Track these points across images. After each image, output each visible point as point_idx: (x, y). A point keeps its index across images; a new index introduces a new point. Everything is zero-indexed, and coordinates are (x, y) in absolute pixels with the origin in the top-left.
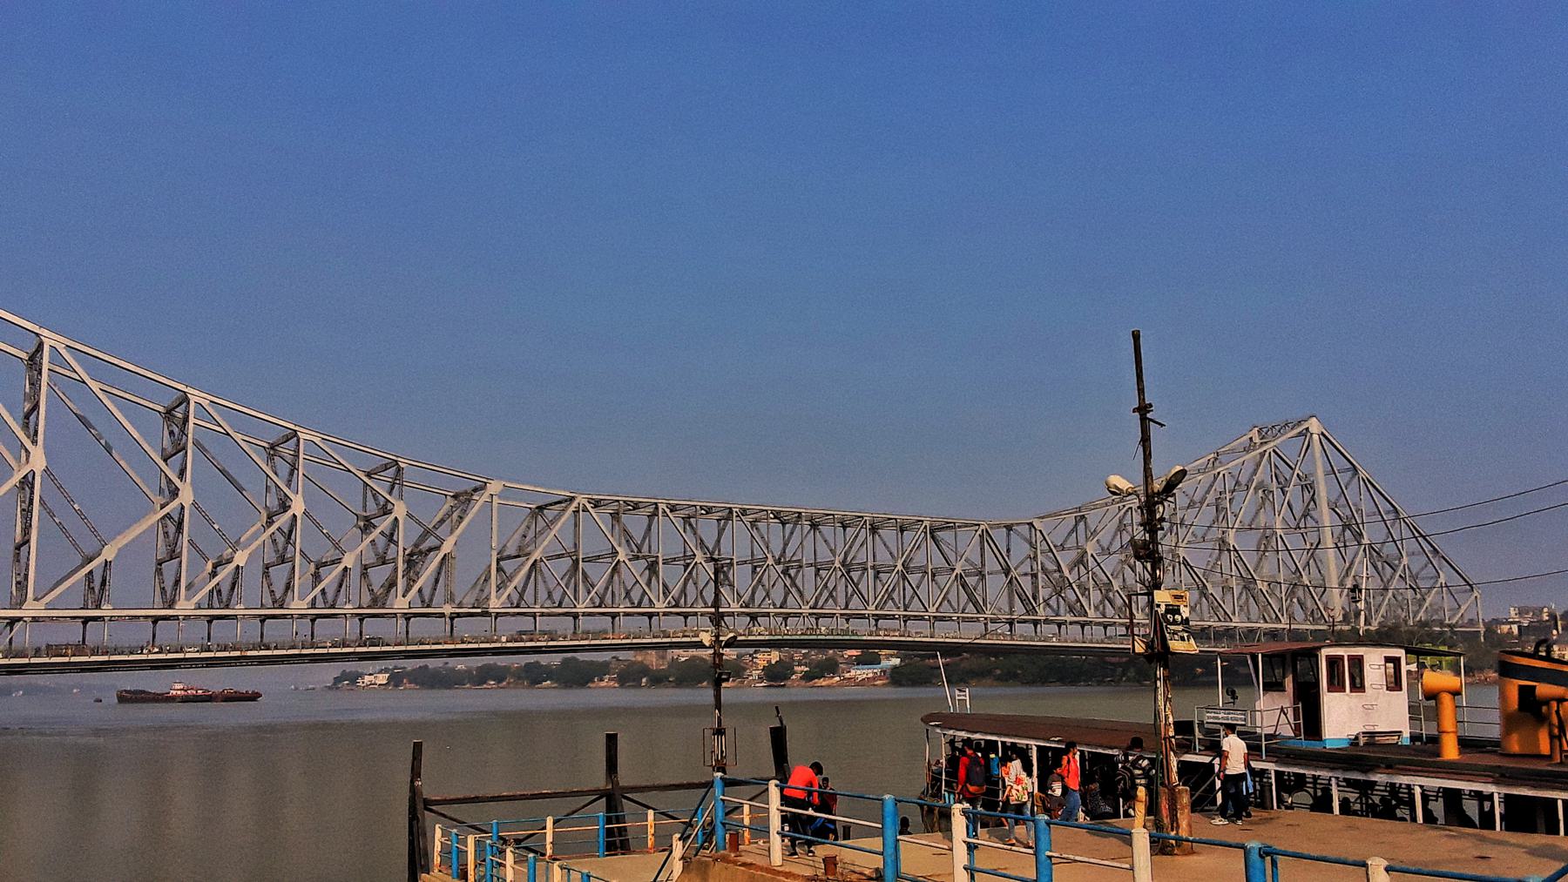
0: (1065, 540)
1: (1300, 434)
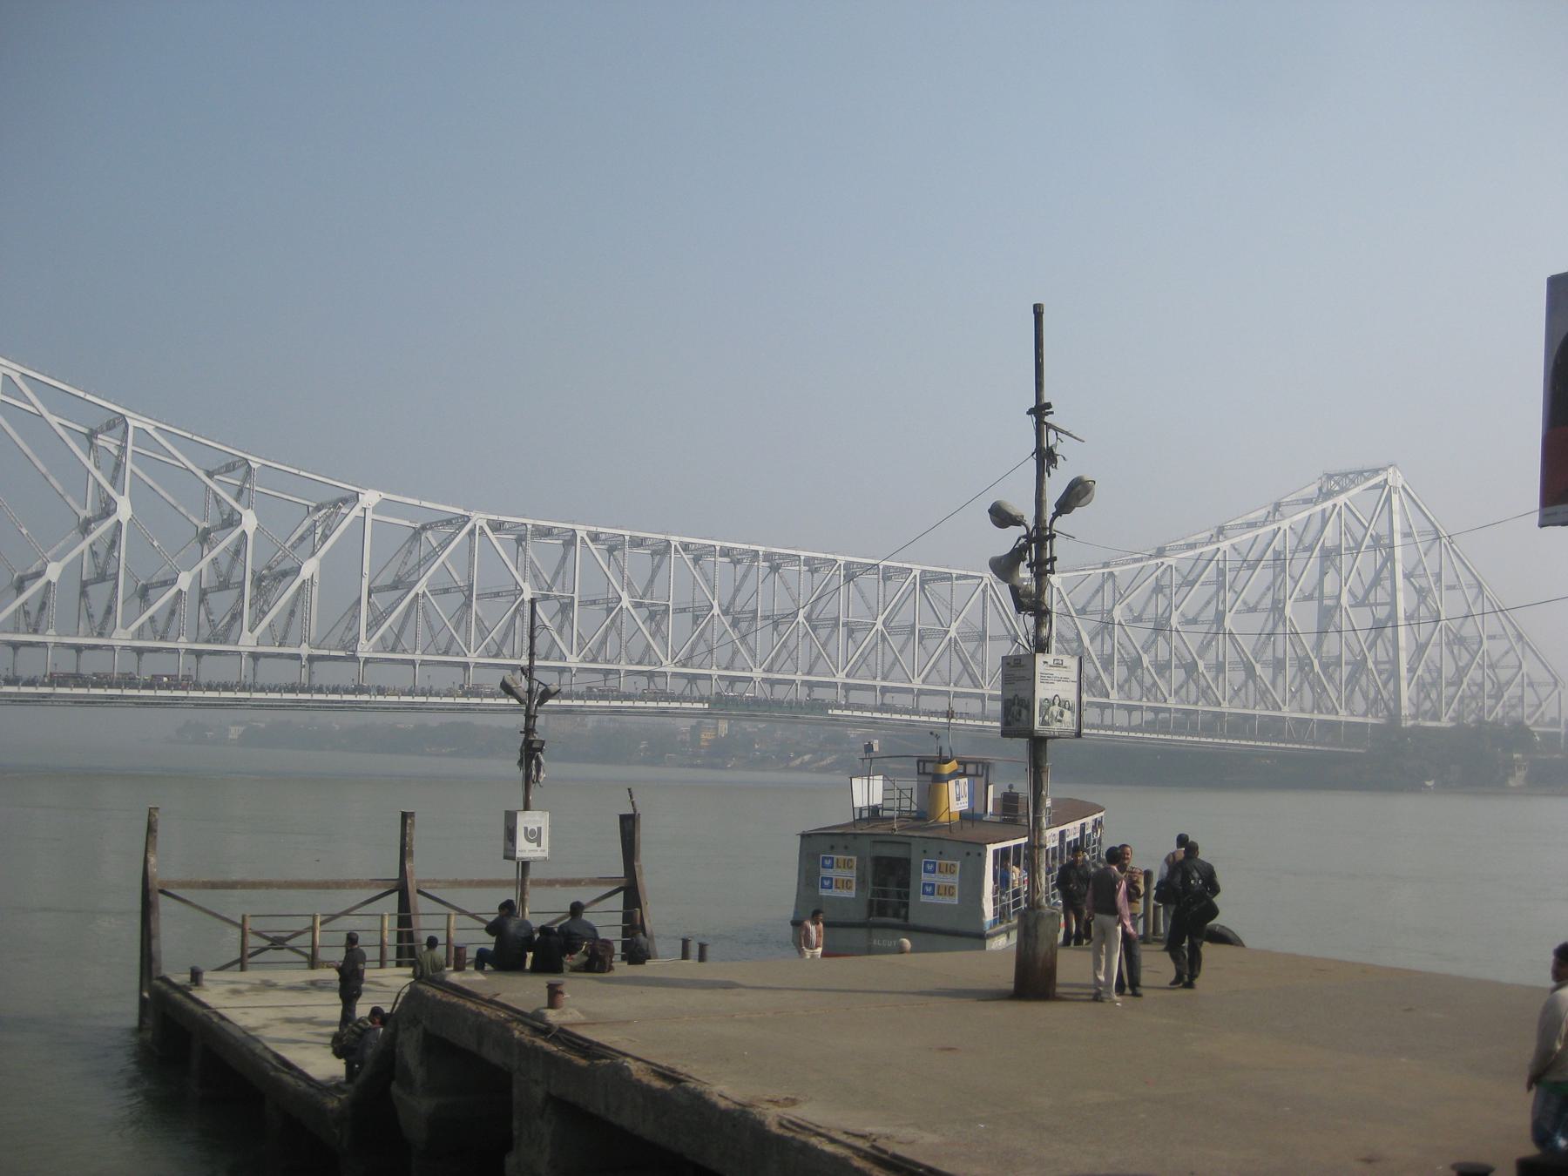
0: (1089, 602)
1: (1375, 487)
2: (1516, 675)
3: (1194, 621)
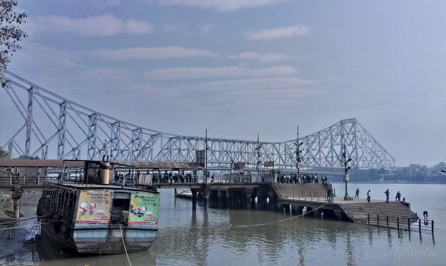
0: (293, 147)
2: (384, 159)
3: (314, 150)
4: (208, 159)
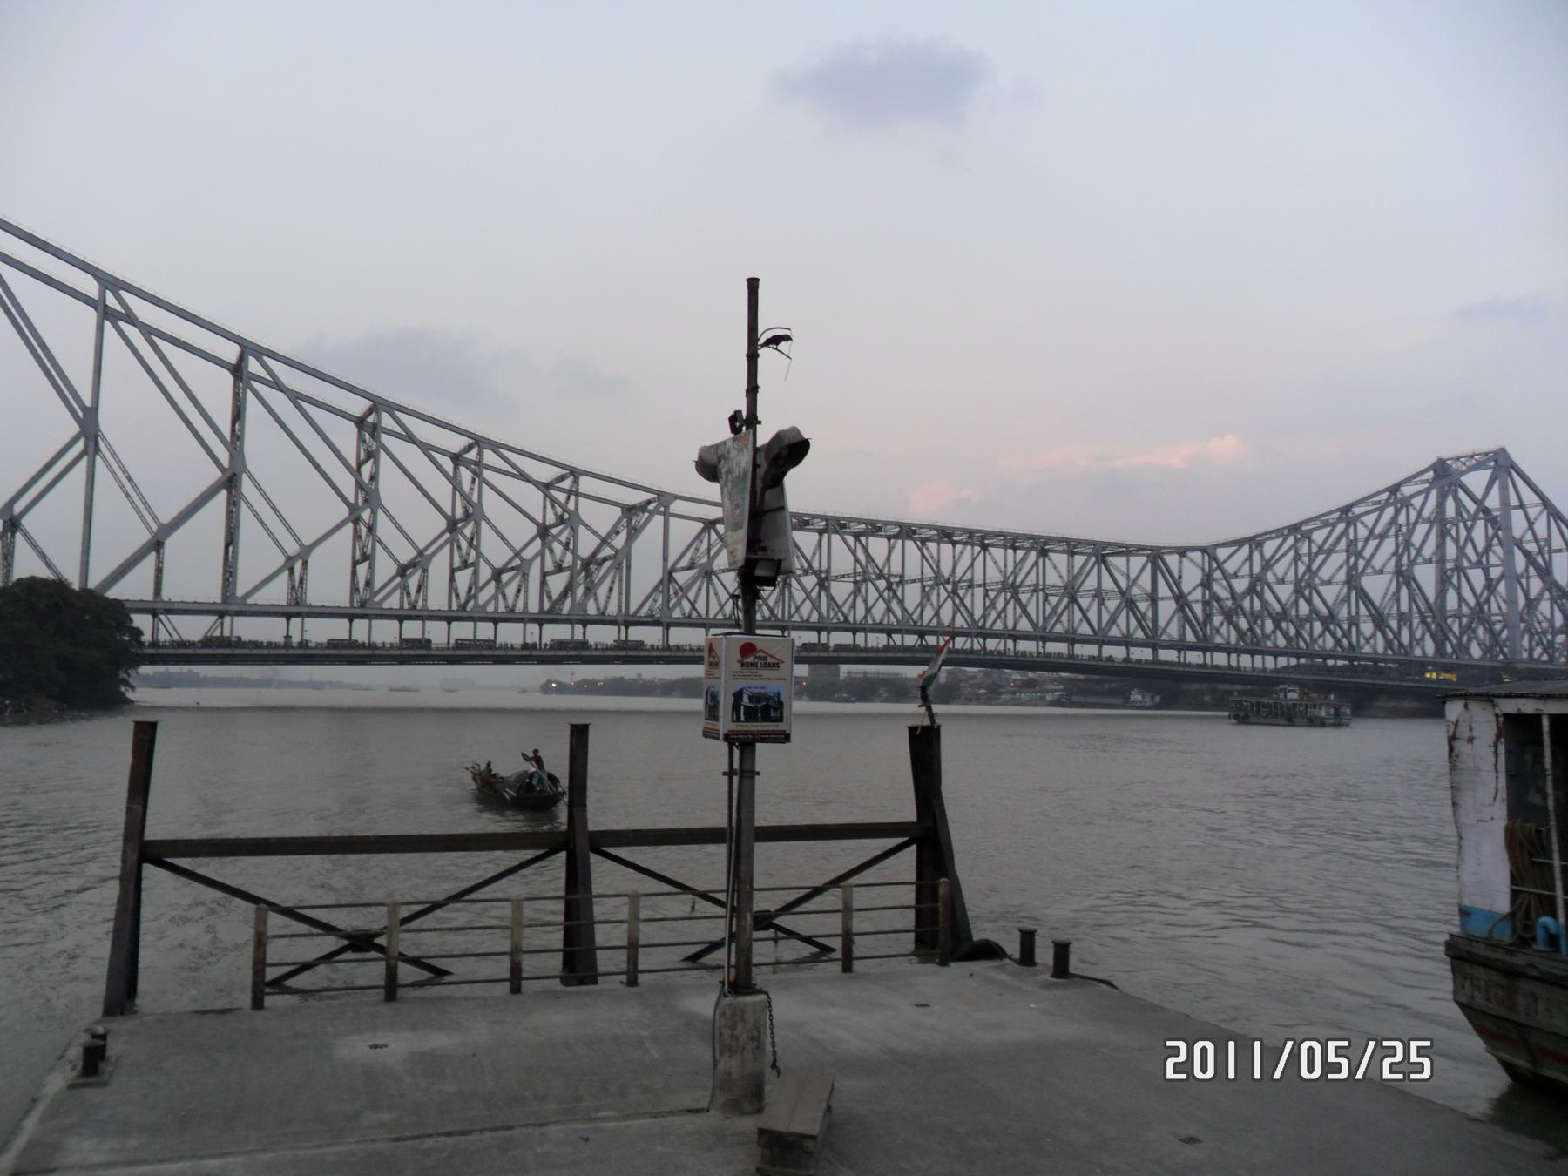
4: (872, 616)
